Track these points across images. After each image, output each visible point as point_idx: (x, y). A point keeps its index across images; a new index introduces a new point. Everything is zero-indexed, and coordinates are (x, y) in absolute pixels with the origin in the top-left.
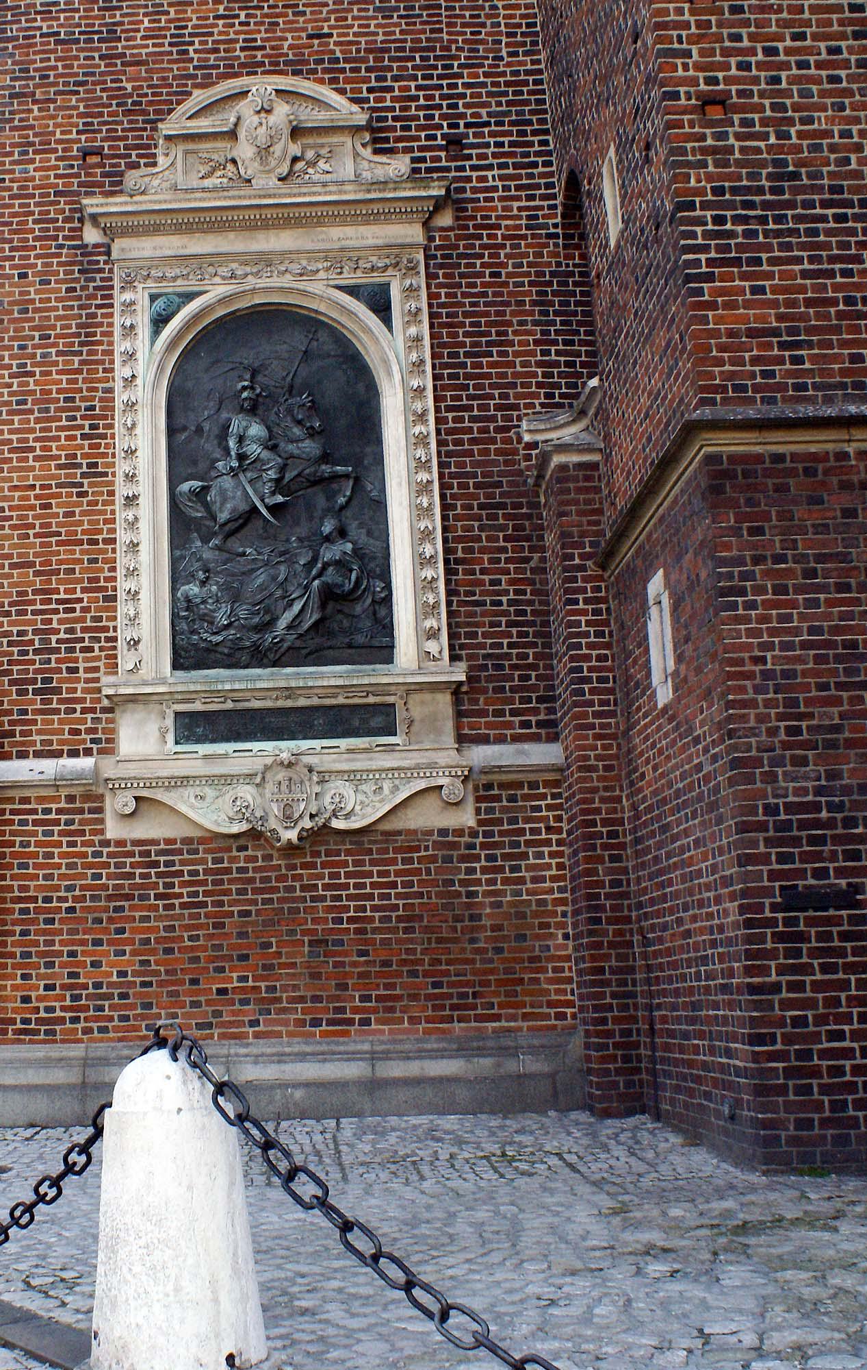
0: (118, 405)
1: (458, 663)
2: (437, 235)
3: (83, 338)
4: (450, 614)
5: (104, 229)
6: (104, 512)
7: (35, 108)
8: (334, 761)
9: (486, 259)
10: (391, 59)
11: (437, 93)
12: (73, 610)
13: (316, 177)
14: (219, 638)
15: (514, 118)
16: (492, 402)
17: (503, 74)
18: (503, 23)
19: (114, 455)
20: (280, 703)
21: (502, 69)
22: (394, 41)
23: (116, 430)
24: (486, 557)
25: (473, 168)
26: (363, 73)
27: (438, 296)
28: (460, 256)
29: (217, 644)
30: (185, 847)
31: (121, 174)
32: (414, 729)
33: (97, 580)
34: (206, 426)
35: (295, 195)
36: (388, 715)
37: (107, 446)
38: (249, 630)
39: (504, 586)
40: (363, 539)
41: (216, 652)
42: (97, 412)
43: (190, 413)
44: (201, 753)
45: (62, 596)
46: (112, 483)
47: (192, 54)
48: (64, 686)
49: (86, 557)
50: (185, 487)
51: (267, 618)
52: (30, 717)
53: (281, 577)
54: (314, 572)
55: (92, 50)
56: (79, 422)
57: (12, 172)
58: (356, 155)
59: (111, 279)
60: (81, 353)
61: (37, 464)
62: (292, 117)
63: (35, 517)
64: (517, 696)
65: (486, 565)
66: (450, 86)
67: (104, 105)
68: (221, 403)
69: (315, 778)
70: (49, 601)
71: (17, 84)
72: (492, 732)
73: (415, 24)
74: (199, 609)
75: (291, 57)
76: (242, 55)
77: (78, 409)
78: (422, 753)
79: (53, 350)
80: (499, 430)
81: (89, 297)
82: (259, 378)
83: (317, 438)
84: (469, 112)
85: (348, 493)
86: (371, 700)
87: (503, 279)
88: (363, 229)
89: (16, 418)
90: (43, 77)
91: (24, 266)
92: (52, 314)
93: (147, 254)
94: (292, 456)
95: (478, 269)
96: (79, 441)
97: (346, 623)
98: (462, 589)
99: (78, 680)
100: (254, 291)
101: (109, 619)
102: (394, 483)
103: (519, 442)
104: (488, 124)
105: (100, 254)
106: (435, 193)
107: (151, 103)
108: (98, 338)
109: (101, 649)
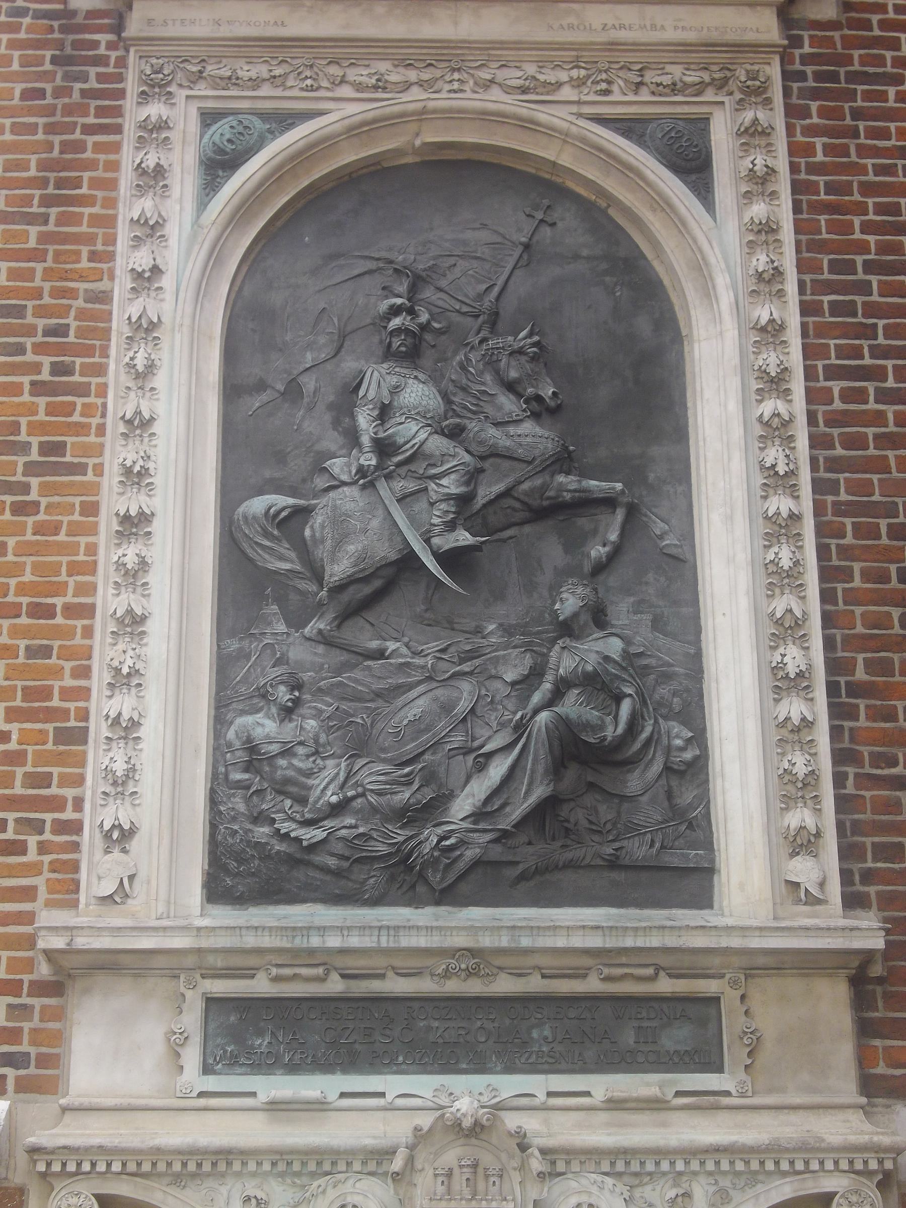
0: (118, 326)
1: (859, 912)
3: (50, 190)
4: (843, 803)
6: (72, 549)
14: (318, 834)
19: (101, 430)
20: (453, 987)
27: (809, 150)
29: (313, 847)
34: (309, 383)
37: (88, 410)
38: (386, 819)
40: (643, 636)
41: (309, 864)
42: (71, 338)
44: (262, 1097)
46: (94, 488)
49: (22, 644)
50: (257, 505)
51: (428, 794)
53: (463, 706)
54: (536, 698)
56: (30, 357)
59: (120, 78)
60: (45, 220)
68: (343, 337)
69: (536, 1164)
74: (274, 768)
77: (30, 331)
78: (783, 1116)
81: (69, 110)
82: (428, 293)
85: (613, 536)
86: (665, 986)
94: (494, 454)
96: (26, 397)
97: (606, 812)
100: (422, 115)
101: (65, 781)
105: (100, 29)
108: (84, 190)
109: (43, 848)
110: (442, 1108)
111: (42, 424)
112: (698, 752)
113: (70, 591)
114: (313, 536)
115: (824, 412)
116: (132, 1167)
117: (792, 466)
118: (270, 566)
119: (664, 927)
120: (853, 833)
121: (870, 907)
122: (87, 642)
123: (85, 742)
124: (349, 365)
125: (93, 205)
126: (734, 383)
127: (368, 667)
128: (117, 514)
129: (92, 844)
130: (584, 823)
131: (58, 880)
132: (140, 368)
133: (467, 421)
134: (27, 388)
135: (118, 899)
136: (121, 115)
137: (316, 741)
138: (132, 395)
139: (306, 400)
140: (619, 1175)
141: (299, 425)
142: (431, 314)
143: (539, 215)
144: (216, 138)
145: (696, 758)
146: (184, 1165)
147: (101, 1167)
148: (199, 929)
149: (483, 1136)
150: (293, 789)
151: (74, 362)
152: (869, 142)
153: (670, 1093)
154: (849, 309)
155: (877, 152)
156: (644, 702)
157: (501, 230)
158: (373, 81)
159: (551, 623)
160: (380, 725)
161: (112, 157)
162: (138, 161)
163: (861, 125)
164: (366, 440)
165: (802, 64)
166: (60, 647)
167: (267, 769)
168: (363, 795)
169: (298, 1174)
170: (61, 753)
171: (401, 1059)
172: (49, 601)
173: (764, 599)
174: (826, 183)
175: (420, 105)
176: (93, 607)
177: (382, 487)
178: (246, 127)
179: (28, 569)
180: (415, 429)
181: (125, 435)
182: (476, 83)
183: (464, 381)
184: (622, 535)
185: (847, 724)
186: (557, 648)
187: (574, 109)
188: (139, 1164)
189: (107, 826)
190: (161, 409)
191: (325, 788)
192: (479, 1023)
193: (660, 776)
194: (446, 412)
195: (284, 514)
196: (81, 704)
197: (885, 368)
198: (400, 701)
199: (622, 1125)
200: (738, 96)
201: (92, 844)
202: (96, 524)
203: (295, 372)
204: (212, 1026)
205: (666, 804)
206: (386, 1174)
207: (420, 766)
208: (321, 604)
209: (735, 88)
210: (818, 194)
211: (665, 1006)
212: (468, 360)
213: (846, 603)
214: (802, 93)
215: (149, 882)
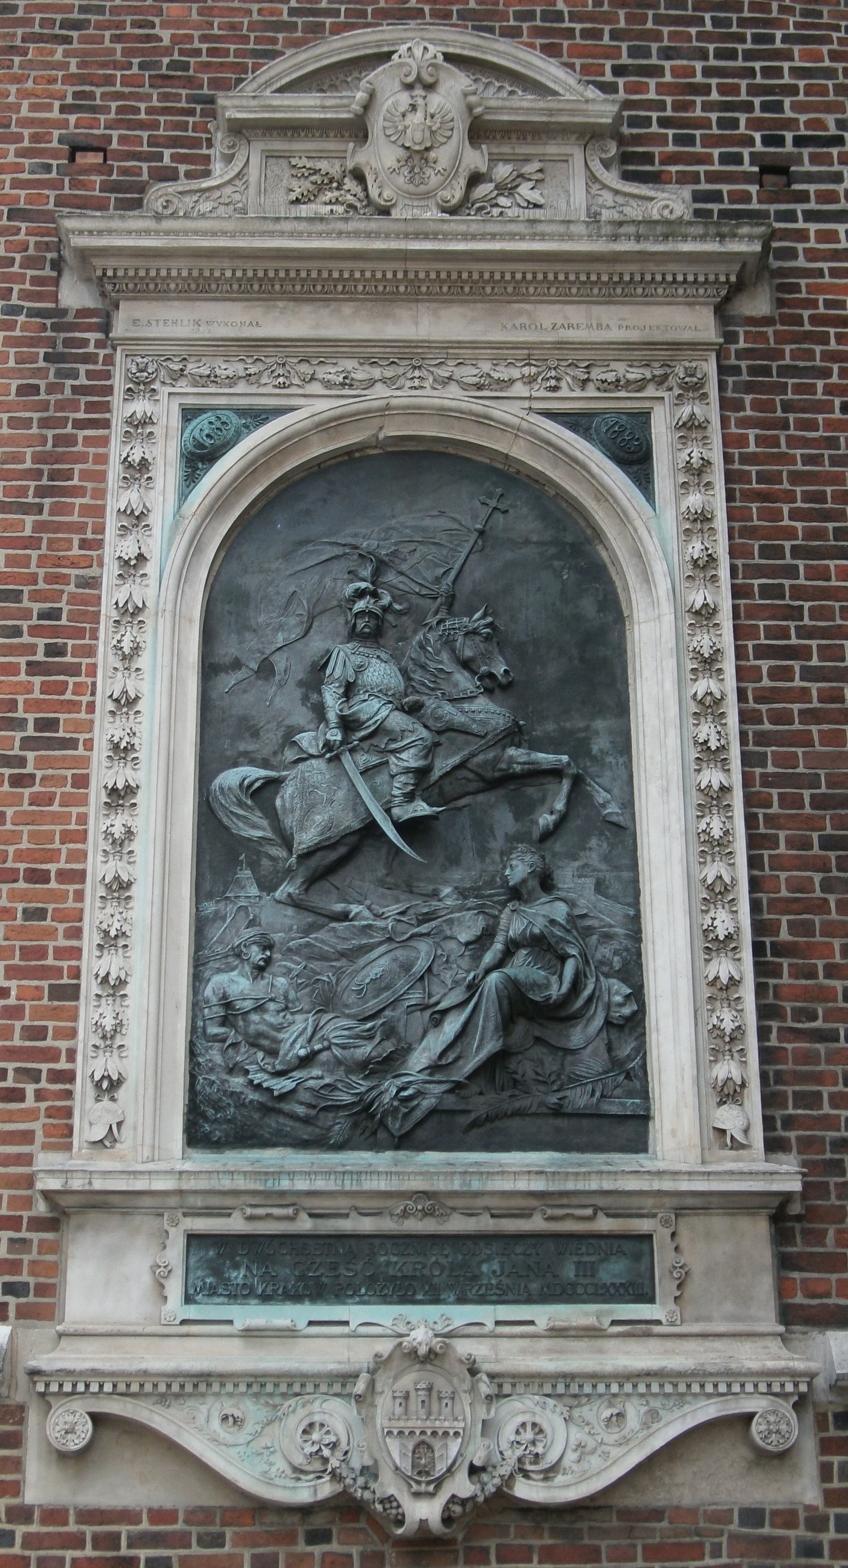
0: (107, 611)
1: (781, 1156)
2: (741, 330)
3: (45, 482)
4: (767, 1055)
6: (64, 818)
8: (523, 1351)
9: (835, 379)
11: (744, 83)
19: (91, 708)
25: (810, 216)
27: (742, 441)
28: (784, 371)
29: (284, 1097)
30: (194, 1530)
31: (142, 188)
33: (41, 953)
34: (280, 662)
35: (473, 237)
36: (637, 1257)
37: (79, 689)
38: (349, 1071)
41: (280, 1112)
42: (64, 621)
43: (248, 635)
44: (239, 1325)
46: (86, 762)
49: (20, 907)
51: (389, 1047)
53: (421, 966)
54: (488, 958)
56: (26, 639)
58: (593, 178)
59: (108, 375)
60: (40, 509)
62: (473, 99)
66: (767, 72)
67: (116, 65)
68: (312, 618)
69: (485, 1388)
77: (26, 614)
78: (709, 1344)
82: (390, 577)
84: (803, 118)
85: (560, 805)
86: (604, 1224)
88: (604, 313)
93: (183, 331)
94: (450, 729)
95: (819, 396)
97: (551, 1064)
98: (788, 1006)
100: (386, 411)
101: (60, 1034)
105: (89, 328)
107: (206, 67)
108: (75, 482)
109: (40, 1095)
110: (401, 1336)
111: (37, 701)
112: (635, 1008)
114: (283, 806)
115: (754, 689)
116: (122, 1388)
117: (723, 742)
118: (243, 833)
119: (601, 1173)
120: (776, 1082)
121: (790, 1151)
122: (79, 905)
123: (76, 998)
124: (316, 645)
126: (672, 663)
127: (333, 928)
128: (106, 787)
129: (83, 1093)
130: (530, 1074)
131: (54, 1126)
132: (127, 650)
133: (424, 698)
134: (23, 667)
135: (107, 1143)
136: (109, 411)
137: (286, 998)
138: (119, 674)
139: (277, 678)
140: (560, 1396)
141: (271, 702)
142: (393, 597)
143: (493, 503)
144: (196, 433)
145: (634, 1014)
146: (169, 1386)
147: (94, 1388)
148: (181, 1173)
149: (436, 1362)
150: (265, 1043)
151: (66, 644)
153: (606, 1322)
154: (776, 592)
155: (805, 443)
156: (587, 962)
157: (458, 517)
158: (341, 379)
159: (502, 887)
160: (344, 983)
161: (101, 450)
162: (124, 455)
163: (791, 417)
164: (332, 716)
166: (54, 910)
167: (241, 1023)
168: (328, 1048)
169: (271, 1395)
170: (55, 1008)
171: (363, 1291)
172: (44, 866)
173: (697, 866)
174: (758, 472)
175: (382, 403)
176: (83, 873)
178: (223, 423)
180: (377, 706)
181: (112, 713)
182: (435, 380)
183: (423, 659)
185: (772, 981)
186: (507, 911)
187: (526, 404)
188: (128, 1386)
189: (97, 1077)
190: (145, 688)
191: (294, 1041)
192: (434, 1259)
193: (601, 1030)
194: (406, 687)
195: (257, 785)
196: (74, 963)
197: (810, 647)
198: (362, 961)
199: (561, 1352)
200: (677, 391)
201: (83, 1093)
202: (87, 795)
203: (268, 652)
204: (192, 1261)
205: (606, 1056)
206: (349, 1395)
207: (381, 1021)
208: (289, 870)
209: (674, 384)
210: (750, 483)
211: (602, 1243)
212: (427, 640)
213: (772, 868)
214: (736, 387)
215: (135, 1128)
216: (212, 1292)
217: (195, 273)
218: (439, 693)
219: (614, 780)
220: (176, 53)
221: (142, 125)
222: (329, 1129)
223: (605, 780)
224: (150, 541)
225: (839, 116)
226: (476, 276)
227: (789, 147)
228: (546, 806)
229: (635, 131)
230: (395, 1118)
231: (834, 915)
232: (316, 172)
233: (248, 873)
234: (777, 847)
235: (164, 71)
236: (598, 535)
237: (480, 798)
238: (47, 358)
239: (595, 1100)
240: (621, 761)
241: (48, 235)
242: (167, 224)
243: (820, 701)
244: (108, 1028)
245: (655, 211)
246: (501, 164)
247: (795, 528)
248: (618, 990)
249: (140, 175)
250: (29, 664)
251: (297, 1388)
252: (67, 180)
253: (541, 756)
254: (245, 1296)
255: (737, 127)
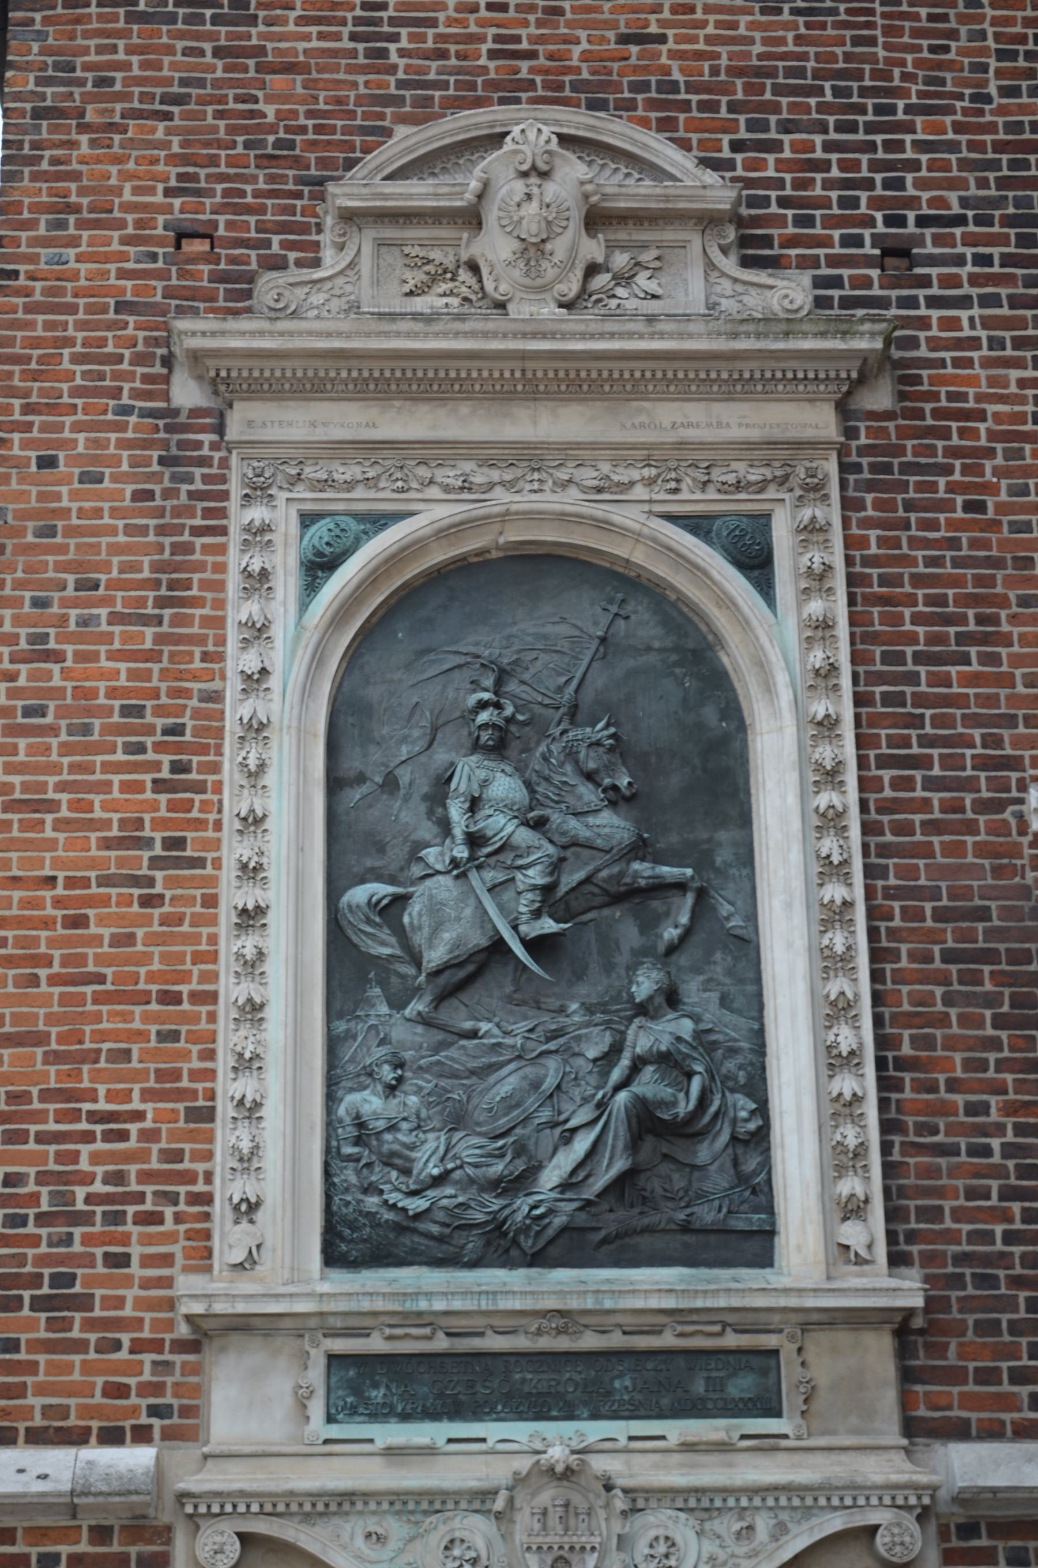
0: (231, 726)
1: (904, 1270)
2: (862, 425)
3: (164, 592)
4: (889, 1169)
5: (214, 382)
6: (196, 939)
7: (84, 139)
8: (656, 1466)
9: (957, 476)
10: (777, 90)
11: (864, 158)
12: (123, 1136)
13: (631, 304)
15: (1011, 210)
16: (969, 752)
17: (992, 128)
18: (990, 31)
19: (218, 825)
20: (545, 1343)
21: (988, 118)
22: (783, 56)
23: (226, 775)
24: (958, 1057)
25: (933, 302)
26: (723, 113)
27: (863, 543)
28: (907, 468)
29: (418, 1216)
32: (819, 1404)
33: (176, 1074)
34: (404, 776)
36: (764, 1372)
37: (205, 807)
38: (482, 1189)
39: (994, 1116)
40: (712, 1013)
41: (415, 1231)
42: (188, 737)
43: (372, 749)
44: (380, 1444)
45: (102, 1105)
46: (213, 881)
47: (394, 58)
48: (99, 1293)
49: (153, 1029)
50: (359, 894)
51: (520, 1165)
52: (22, 1356)
53: (549, 1083)
54: (616, 1075)
55: (197, 36)
56: (150, 756)
57: (33, 259)
58: (710, 265)
59: (223, 479)
61: (61, 836)
62: (589, 188)
63: (52, 943)
64: (1024, 1341)
65: (959, 1073)
66: (889, 146)
67: (220, 144)
68: (435, 730)
69: (620, 1503)
70: (74, 1116)
71: (49, 90)
72: (974, 1416)
73: (823, 26)
75: (585, 75)
76: (492, 65)
77: (150, 730)
78: (834, 1457)
79: (103, 612)
80: (983, 806)
81: (177, 512)
82: (512, 686)
83: (623, 807)
84: (925, 195)
85: (684, 919)
86: (731, 1340)
87: (991, 514)
89: (22, 743)
90: (100, 82)
91: (49, 444)
92: (104, 540)
93: (298, 433)
94: (575, 844)
95: (941, 494)
96: (149, 795)
97: (679, 1181)
98: (910, 1120)
99: (127, 1282)
100: (505, 517)
101: (196, 1156)
102: (777, 904)
103: (1023, 831)
104: (960, 220)
105: (203, 429)
106: (862, 344)
107: (313, 145)
108: (194, 592)
109: (178, 1218)
111: (164, 820)
112: (760, 1122)
113: (195, 978)
115: (876, 800)
116: (268, 1508)
118: (372, 951)
119: (729, 1290)
120: (899, 1197)
122: (211, 1027)
123: (212, 1119)
124: (441, 756)
125: (203, 606)
126: (793, 777)
127: (463, 1047)
130: (659, 1191)
132: (253, 768)
134: (149, 785)
136: (226, 517)
137: (418, 1117)
138: (246, 792)
139: (402, 792)
140: (692, 1510)
143: (614, 609)
144: (316, 541)
145: (760, 1129)
146: (314, 1505)
147: (242, 1508)
148: (321, 1295)
150: (397, 1161)
152: (920, 533)
153: (736, 1436)
154: (899, 700)
155: (927, 544)
157: (579, 623)
158: (460, 483)
160: (475, 1101)
161: (219, 559)
163: (913, 516)
164: (458, 832)
165: (859, 455)
166: (188, 1032)
167: (374, 1143)
168: (461, 1167)
169: (412, 1512)
170: (191, 1131)
172: (176, 988)
175: (502, 508)
177: (473, 876)
179: (156, 958)
180: (503, 821)
181: (240, 832)
184: (693, 918)
185: (894, 1096)
187: (646, 507)
188: (274, 1506)
189: (236, 1200)
190: (272, 805)
195: (385, 902)
196: (208, 1085)
197: (931, 756)
198: (493, 1078)
199: (693, 1466)
200: (798, 492)
201: (223, 1216)
202: (216, 915)
204: (334, 1380)
205: (732, 1171)
206: (489, 1511)
208: (419, 988)
210: (871, 586)
211: (731, 1358)
212: (550, 751)
213: (894, 982)
215: (274, 1250)
216: (353, 1412)
217: (310, 373)
218: (563, 806)
219: (738, 892)
220: (281, 130)
221: (249, 210)
222: (463, 1247)
223: (728, 893)
224: (272, 654)
225: (963, 193)
226: (594, 375)
227: (911, 228)
228: (670, 921)
229: (754, 212)
230: (527, 1236)
231: (955, 1029)
232: (429, 262)
233: (377, 991)
234: (898, 959)
235: (269, 150)
236: (720, 641)
237: (606, 912)
238: (162, 461)
239: (721, 1215)
240: (744, 872)
241: (157, 329)
242: (282, 325)
243: (942, 811)
244: (245, 1151)
245: (775, 301)
246: (617, 252)
247: (916, 633)
248: (744, 1104)
249: (248, 264)
250: (155, 781)
251: (437, 1506)
252: (174, 269)
253: (665, 869)
254: (385, 1415)
255: (857, 207)
